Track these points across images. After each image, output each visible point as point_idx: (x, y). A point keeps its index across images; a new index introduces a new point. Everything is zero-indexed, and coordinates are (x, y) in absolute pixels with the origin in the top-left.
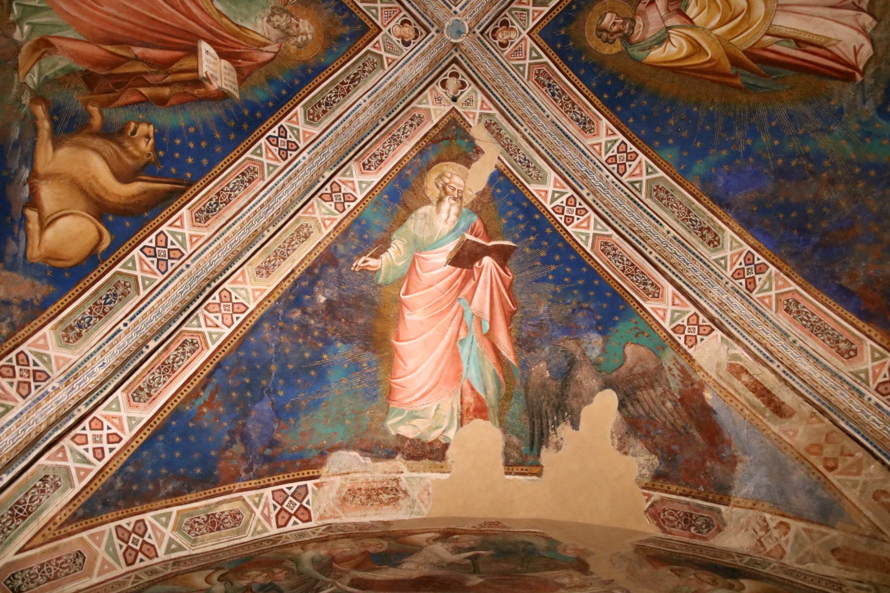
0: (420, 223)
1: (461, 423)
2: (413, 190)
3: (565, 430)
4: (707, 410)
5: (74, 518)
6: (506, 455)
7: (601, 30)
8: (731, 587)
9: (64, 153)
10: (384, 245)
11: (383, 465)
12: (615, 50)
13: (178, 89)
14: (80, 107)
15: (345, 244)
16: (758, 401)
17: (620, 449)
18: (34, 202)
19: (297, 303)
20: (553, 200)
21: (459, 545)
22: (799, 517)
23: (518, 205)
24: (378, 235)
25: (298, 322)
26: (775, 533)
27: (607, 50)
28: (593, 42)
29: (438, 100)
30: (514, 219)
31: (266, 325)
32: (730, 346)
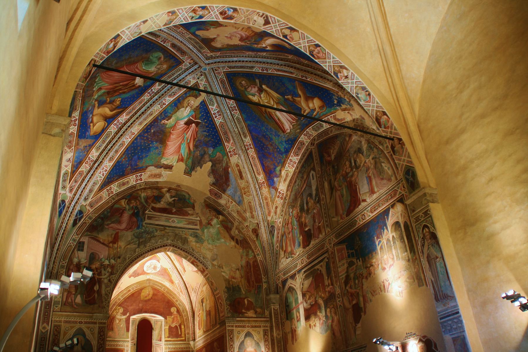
0: (180, 113)
1: (177, 162)
2: (180, 103)
3: (199, 168)
4: (228, 173)
5: (100, 190)
6: (185, 171)
7: (241, 83)
8: (217, 218)
9: (100, 109)
10: (170, 118)
11: (159, 170)
12: (242, 89)
13: (129, 89)
14: (105, 99)
15: (161, 117)
16: (238, 174)
17: (208, 175)
18: (92, 122)
19: (147, 132)
20: (214, 111)
21: (172, 194)
22: (235, 202)
23: (205, 111)
24: (169, 115)
25: (146, 137)
26: (230, 203)
27: (240, 88)
28: (238, 84)
29: (194, 78)
30: (203, 114)
31: (139, 138)
32: (238, 159)
